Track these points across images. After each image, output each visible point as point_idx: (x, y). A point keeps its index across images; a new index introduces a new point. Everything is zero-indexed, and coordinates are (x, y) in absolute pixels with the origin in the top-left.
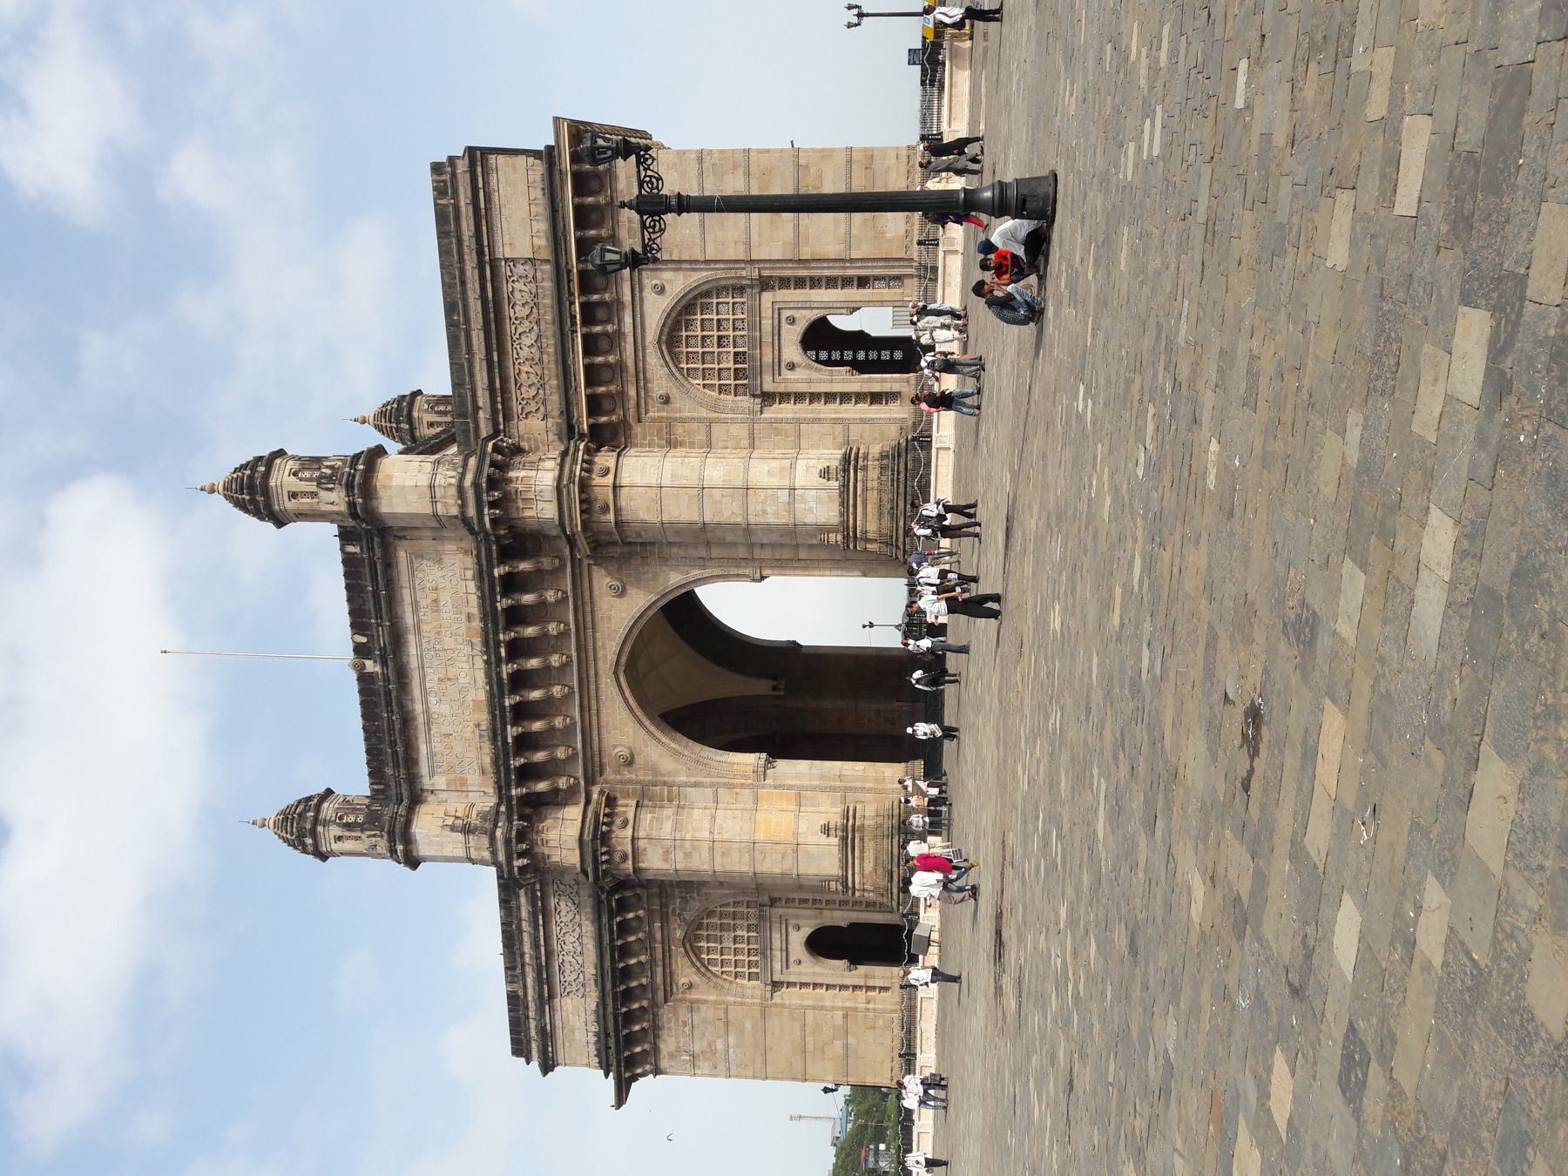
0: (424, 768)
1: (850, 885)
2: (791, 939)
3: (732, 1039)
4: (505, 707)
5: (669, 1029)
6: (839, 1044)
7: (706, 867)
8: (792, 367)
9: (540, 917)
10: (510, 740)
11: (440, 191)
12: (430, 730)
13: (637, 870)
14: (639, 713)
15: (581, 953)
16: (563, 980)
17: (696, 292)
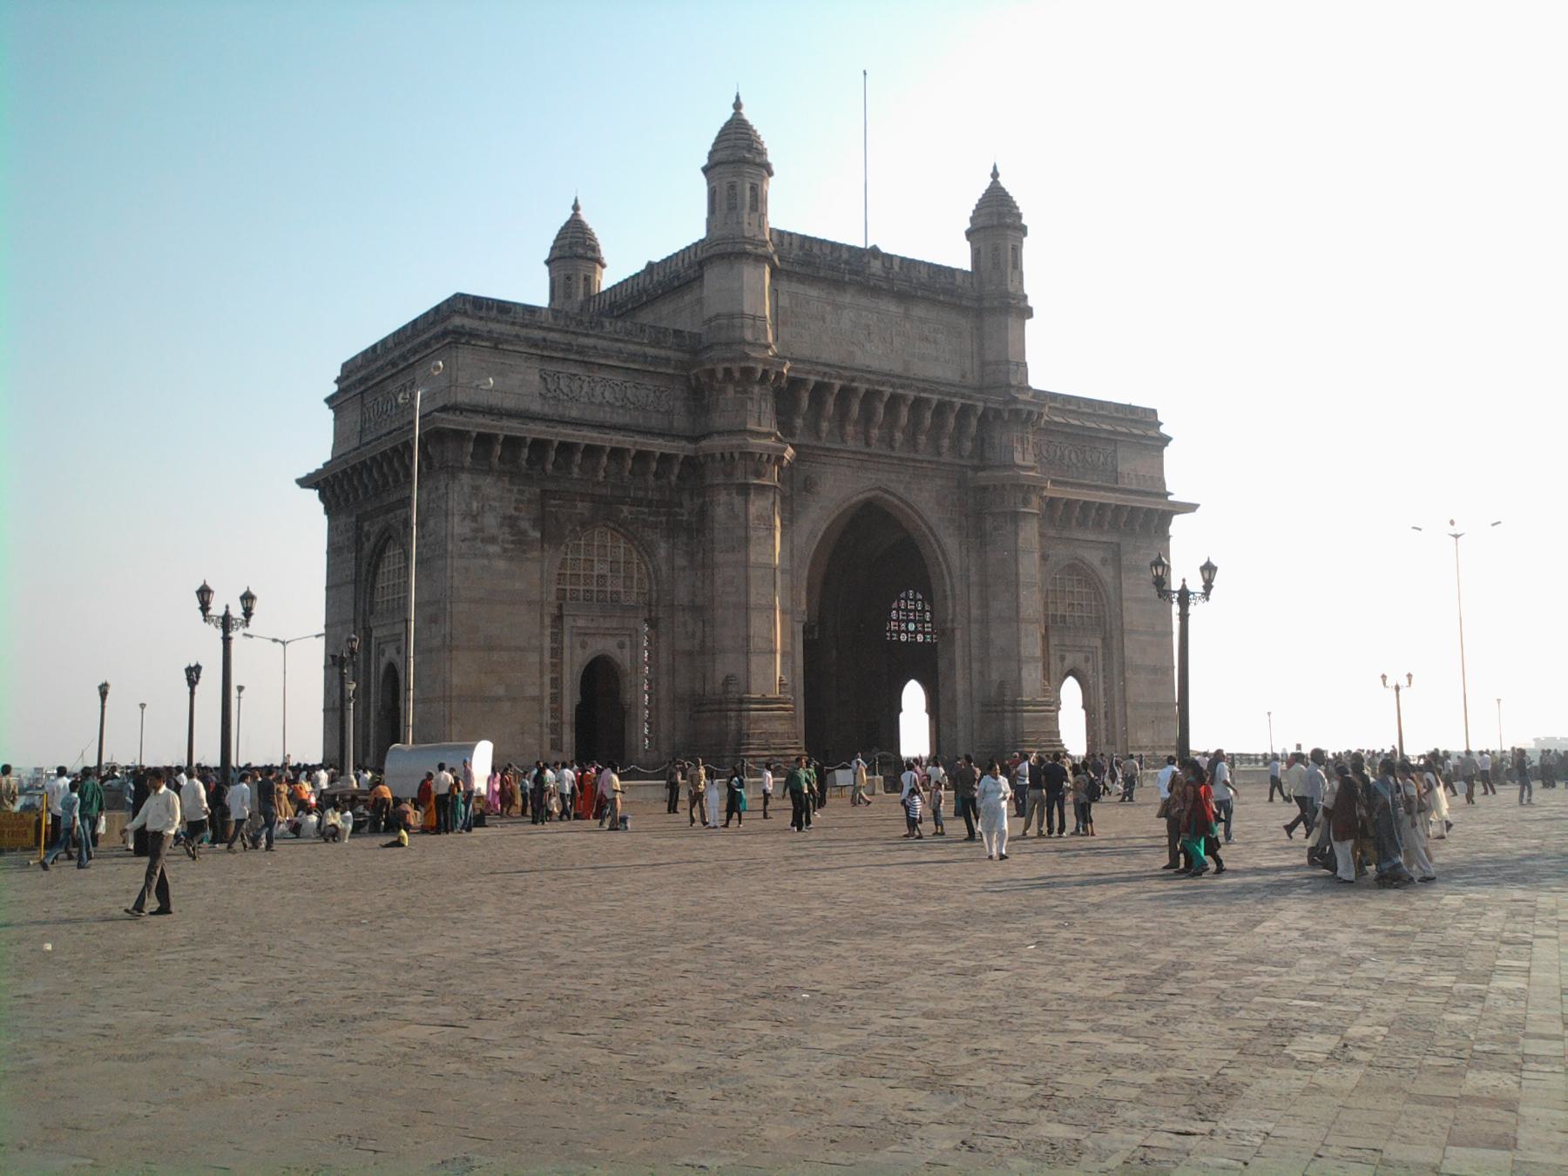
0: (796, 287)
1: (745, 706)
2: (609, 637)
3: (501, 564)
4: (883, 384)
5: (510, 491)
6: (501, 691)
7: (752, 558)
8: (1063, 659)
9: (636, 367)
10: (855, 384)
11: (1145, 410)
12: (829, 304)
13: (744, 490)
14: (845, 505)
15: (592, 403)
16: (561, 375)
17: (1101, 590)
